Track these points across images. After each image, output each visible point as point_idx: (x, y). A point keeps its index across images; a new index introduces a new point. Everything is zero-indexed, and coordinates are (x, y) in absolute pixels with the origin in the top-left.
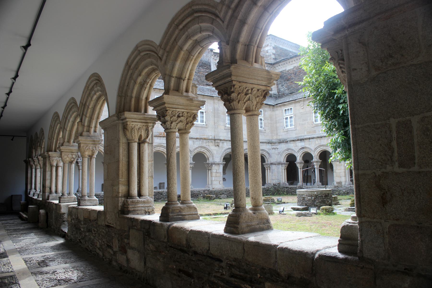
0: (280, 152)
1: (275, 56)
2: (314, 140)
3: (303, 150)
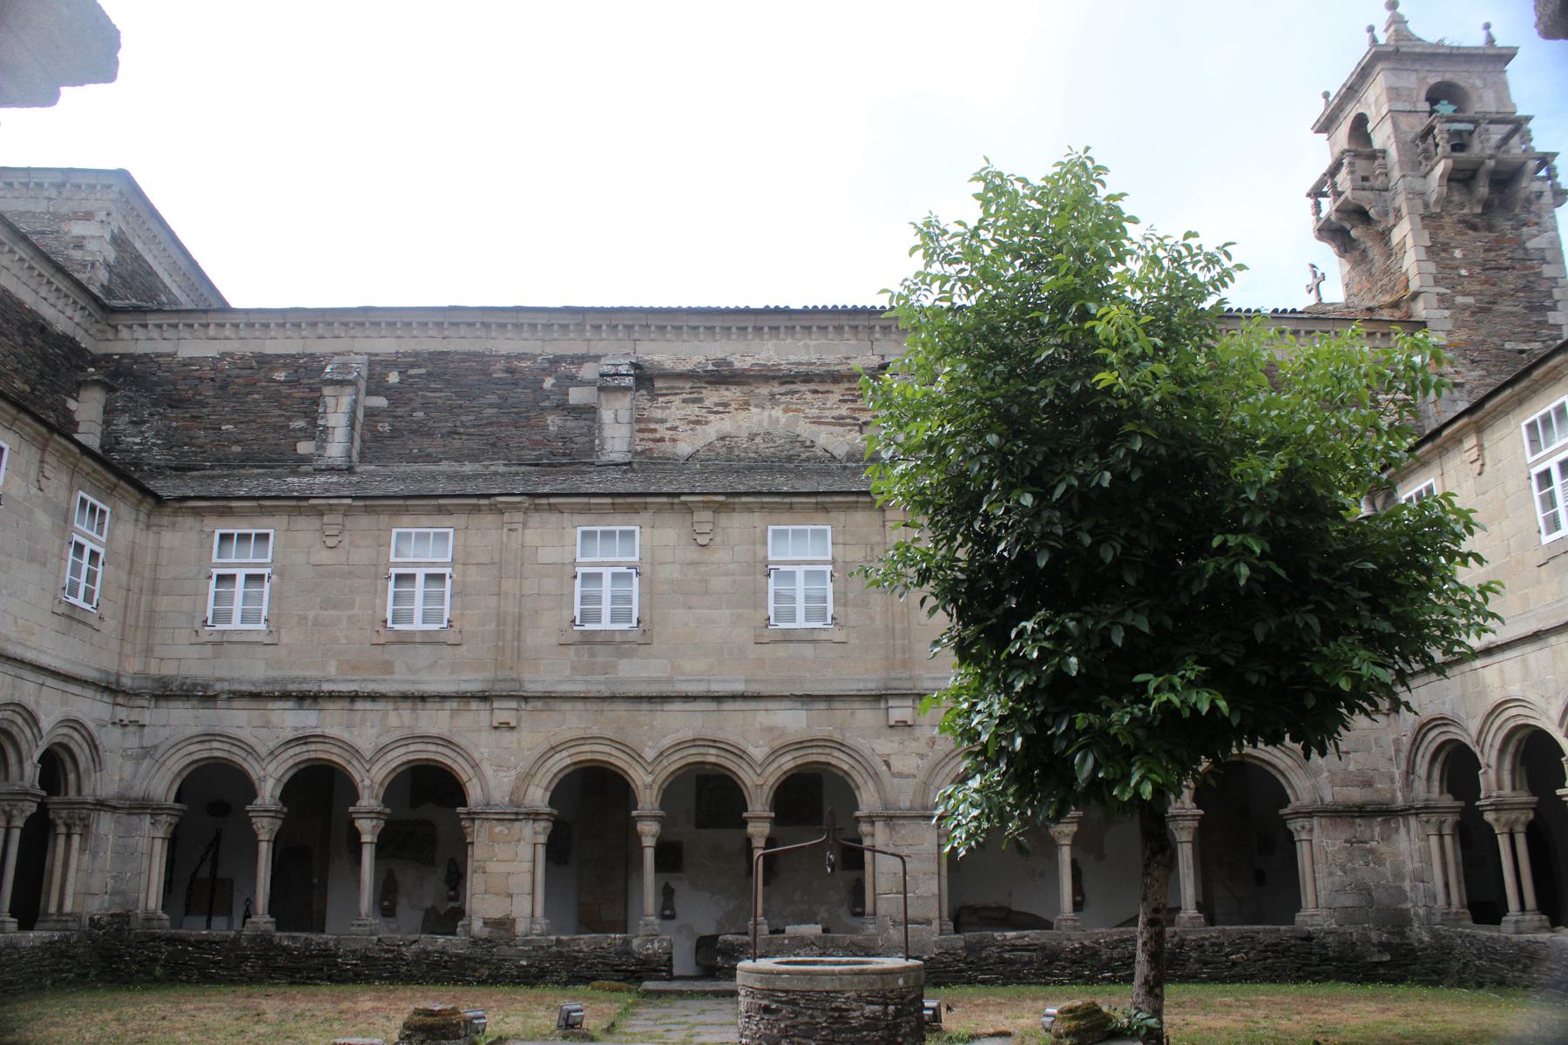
0: (155, 747)
1: (110, 281)
2: (380, 705)
3: (305, 748)
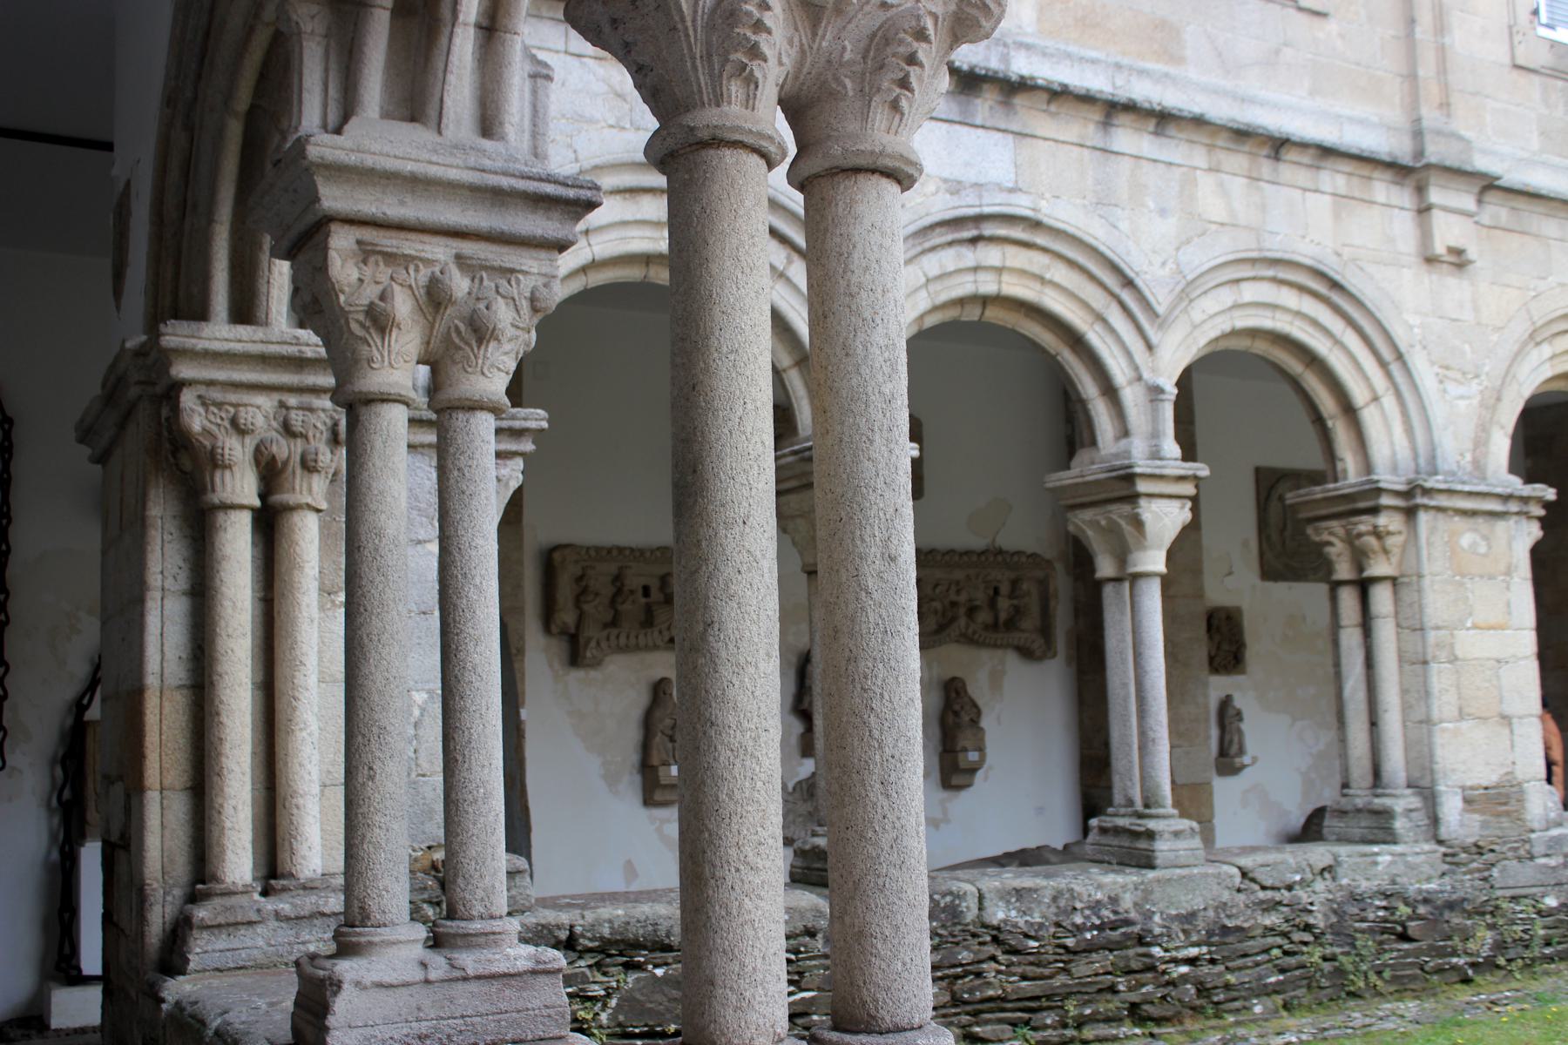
2: (1177, 150)
3: (969, 256)
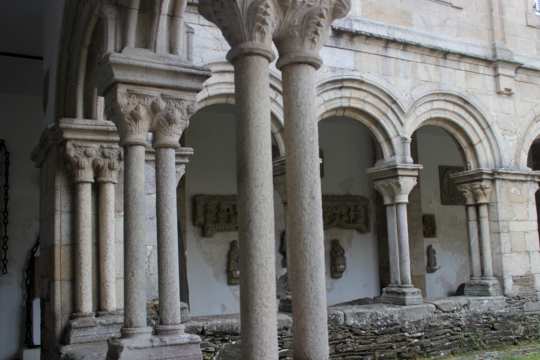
2: (410, 56)
3: (339, 93)
